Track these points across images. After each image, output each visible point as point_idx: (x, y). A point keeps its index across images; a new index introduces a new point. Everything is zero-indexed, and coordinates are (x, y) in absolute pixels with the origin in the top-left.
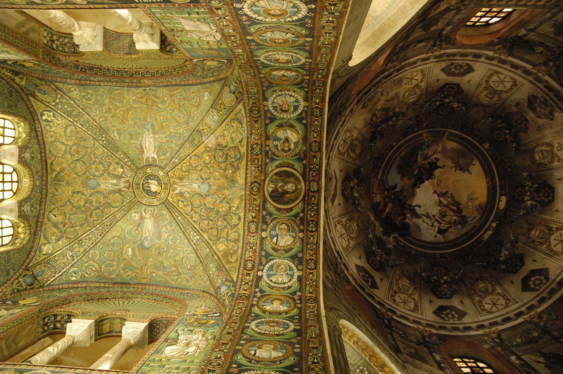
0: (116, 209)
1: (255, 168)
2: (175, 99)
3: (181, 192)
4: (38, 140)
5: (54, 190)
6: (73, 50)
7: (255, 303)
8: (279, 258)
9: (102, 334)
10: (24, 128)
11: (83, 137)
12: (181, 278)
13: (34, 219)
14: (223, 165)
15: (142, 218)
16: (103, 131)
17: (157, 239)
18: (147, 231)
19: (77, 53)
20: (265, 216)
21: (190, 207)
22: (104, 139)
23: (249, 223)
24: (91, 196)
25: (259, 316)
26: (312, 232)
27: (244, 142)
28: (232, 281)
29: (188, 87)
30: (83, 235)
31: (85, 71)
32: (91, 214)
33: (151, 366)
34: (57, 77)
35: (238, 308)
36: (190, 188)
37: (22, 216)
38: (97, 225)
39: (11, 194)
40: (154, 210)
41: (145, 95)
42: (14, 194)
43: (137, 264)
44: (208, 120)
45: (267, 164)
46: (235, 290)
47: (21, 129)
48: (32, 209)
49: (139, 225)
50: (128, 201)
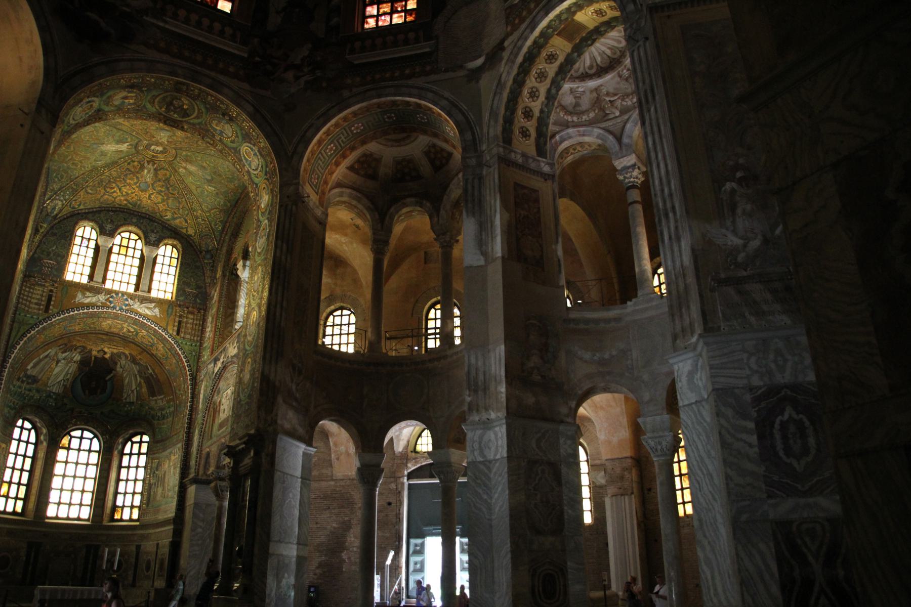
0: (173, 177)
3: (168, 142)
4: (96, 211)
5: (144, 209)
11: (99, 183)
13: (165, 231)
15: (185, 168)
16: (95, 168)
24: (155, 190)
32: (172, 194)
37: (156, 244)
39: (139, 241)
42: (140, 238)
47: (85, 224)
48: (155, 231)
49: (190, 173)
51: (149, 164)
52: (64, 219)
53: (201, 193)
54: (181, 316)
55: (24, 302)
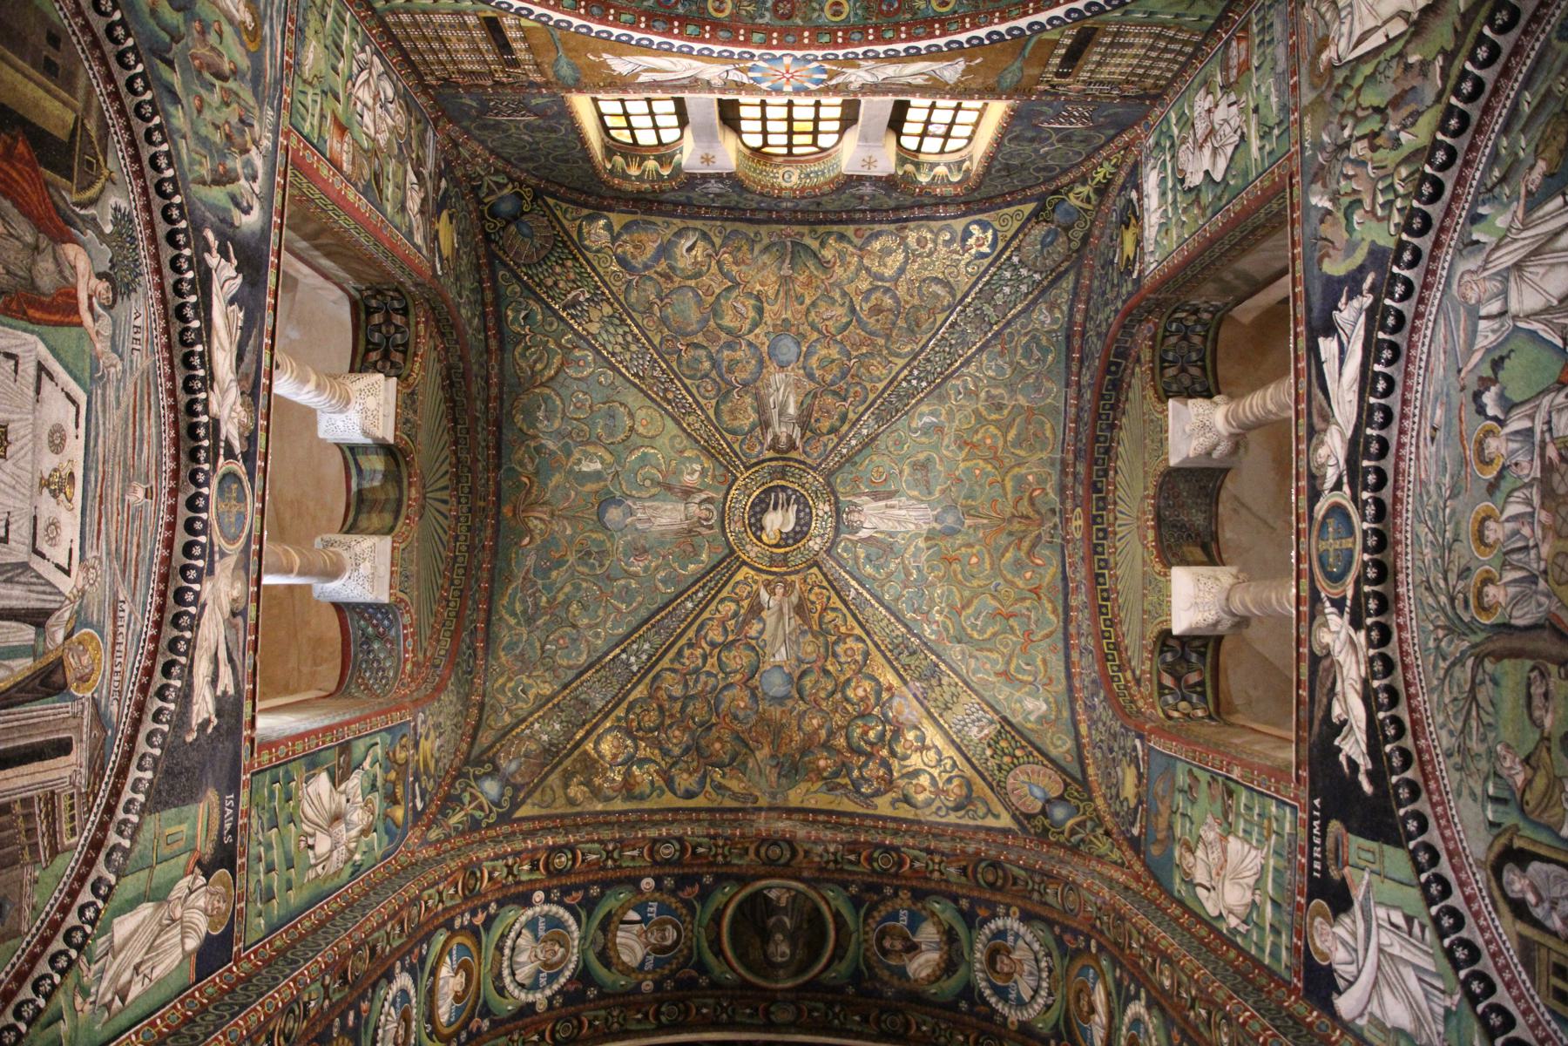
1: (835, 854)
2: (1028, 603)
3: (761, 609)
4: (912, 207)
5: (766, 241)
6: (1170, 356)
7: (457, 923)
8: (583, 938)
9: (353, 454)
10: (946, 181)
11: (918, 325)
12: (518, 623)
13: (683, 199)
14: (841, 741)
15: (687, 493)
16: (937, 387)
17: (627, 544)
18: (649, 512)
19: (1163, 369)
20: (700, 882)
21: (720, 639)
22: (914, 382)
23: (680, 840)
24: (750, 344)
25: (422, 970)
26: (657, 1014)
27: (904, 812)
28: (515, 805)
29: (1060, 645)
30: (637, 326)
31: (1108, 372)
32: (697, 346)
33: (272, 794)
34: (1091, 280)
35: (440, 893)
36: (775, 636)
38: (665, 361)
40: (711, 527)
41: (1038, 512)
42: (756, 151)
43: (557, 487)
44: (968, 701)
45: (845, 885)
46: (489, 826)
47: (941, 170)
49: (669, 488)
50: (736, 447)
51: (789, 437)
52: (1010, 193)
53: (613, 417)
54: (516, 63)
55: (1177, 47)
